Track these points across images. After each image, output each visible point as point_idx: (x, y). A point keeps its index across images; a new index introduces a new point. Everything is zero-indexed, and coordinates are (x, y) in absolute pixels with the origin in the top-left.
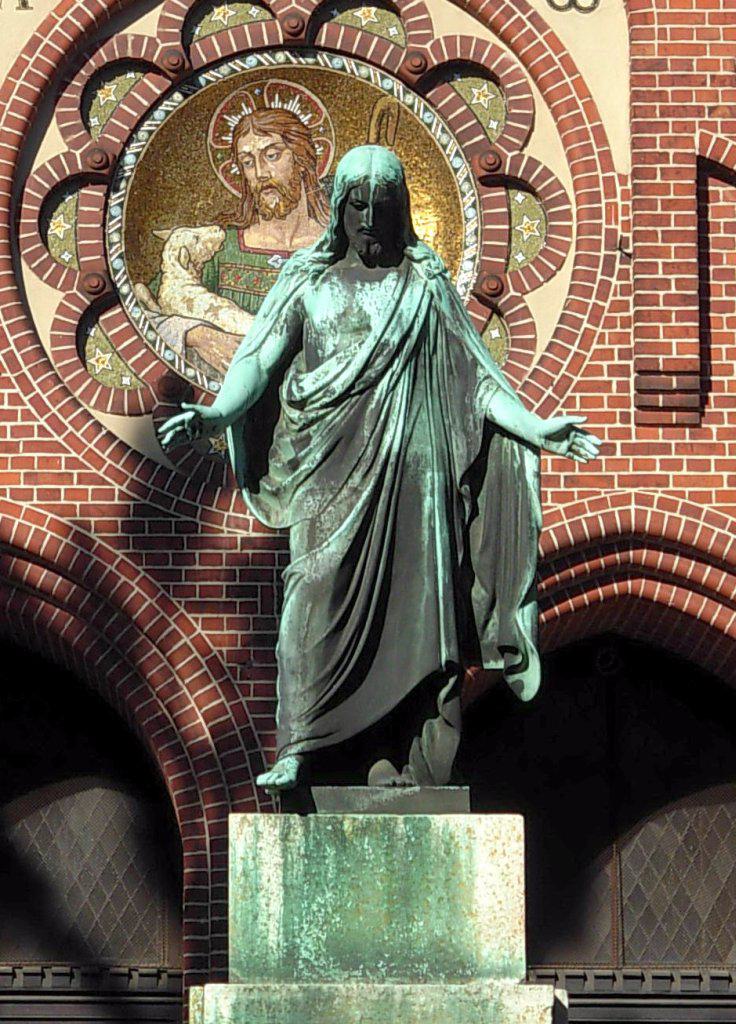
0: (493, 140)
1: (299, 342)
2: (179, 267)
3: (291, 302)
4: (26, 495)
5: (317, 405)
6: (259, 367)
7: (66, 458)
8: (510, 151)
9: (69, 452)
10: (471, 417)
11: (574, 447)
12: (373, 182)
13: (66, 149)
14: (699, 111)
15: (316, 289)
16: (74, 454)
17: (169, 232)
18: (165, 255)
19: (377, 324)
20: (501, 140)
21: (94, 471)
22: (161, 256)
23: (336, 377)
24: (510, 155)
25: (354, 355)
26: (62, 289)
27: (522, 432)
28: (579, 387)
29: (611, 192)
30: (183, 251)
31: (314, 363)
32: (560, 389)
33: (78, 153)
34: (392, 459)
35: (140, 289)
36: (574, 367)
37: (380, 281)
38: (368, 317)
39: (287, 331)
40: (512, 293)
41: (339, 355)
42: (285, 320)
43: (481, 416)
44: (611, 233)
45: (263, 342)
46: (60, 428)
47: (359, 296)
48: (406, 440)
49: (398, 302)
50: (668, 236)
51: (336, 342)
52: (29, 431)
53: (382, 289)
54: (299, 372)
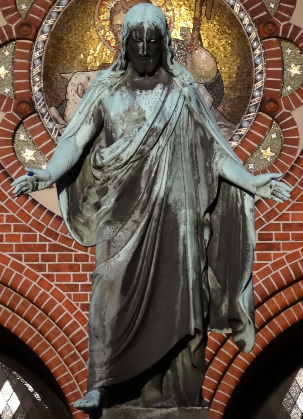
0: (272, 15)
1: (102, 129)
2: (78, 97)
3: (96, 103)
5: (112, 168)
6: (76, 145)
7: (7, 216)
8: (282, 21)
9: (8, 212)
10: (210, 175)
11: (275, 193)
12: (146, 26)
13: (5, 23)
15: (112, 95)
16: (11, 213)
17: (71, 74)
18: (69, 89)
19: (150, 116)
20: (277, 15)
21: (24, 223)
22: (66, 90)
23: (123, 151)
24: (282, 24)
25: (135, 136)
26: (5, 110)
27: (241, 183)
30: (80, 87)
31: (110, 141)
33: (13, 26)
34: (159, 202)
35: (53, 111)
37: (152, 89)
38: (144, 112)
39: (94, 121)
40: (284, 110)
41: (125, 136)
42: (93, 115)
43: (216, 174)
45: (79, 129)
47: (138, 99)
48: (168, 191)
49: (164, 102)
51: (124, 128)
53: (153, 94)
54: (101, 147)
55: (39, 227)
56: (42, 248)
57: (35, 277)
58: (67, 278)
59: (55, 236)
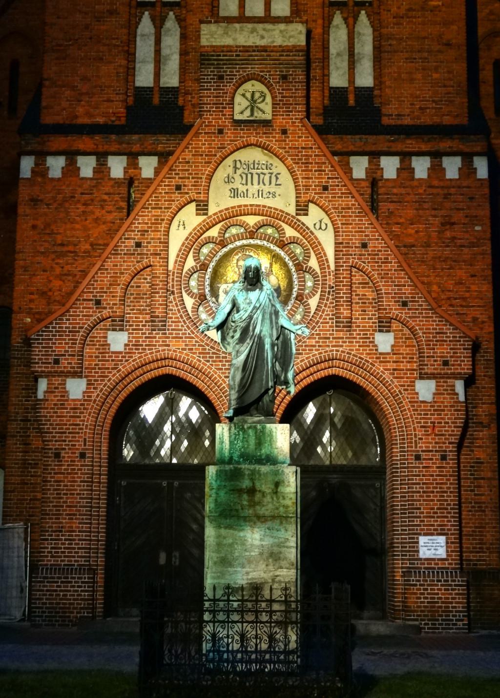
4: (185, 349)
14: (351, 255)
28: (322, 323)
29: (330, 275)
32: (317, 323)
36: (320, 318)
44: (330, 285)
46: (193, 333)
50: (344, 286)
52: (186, 334)
55: (208, 345)
56: (209, 353)
57: (206, 365)
58: (219, 365)
59: (214, 348)
